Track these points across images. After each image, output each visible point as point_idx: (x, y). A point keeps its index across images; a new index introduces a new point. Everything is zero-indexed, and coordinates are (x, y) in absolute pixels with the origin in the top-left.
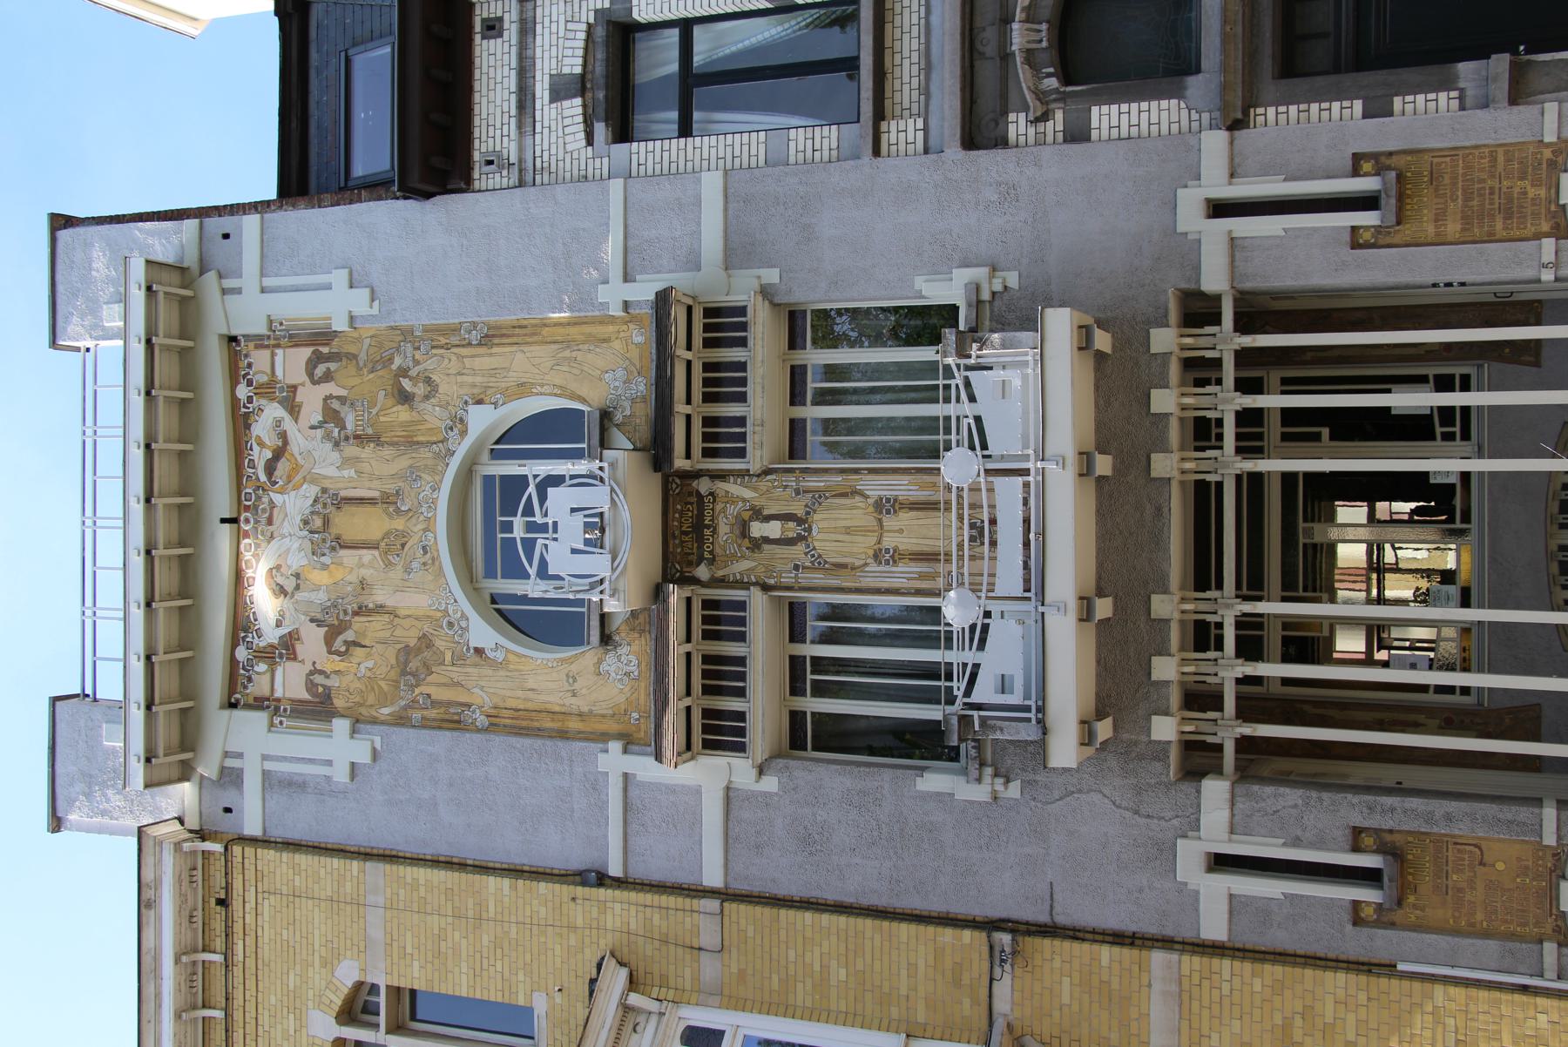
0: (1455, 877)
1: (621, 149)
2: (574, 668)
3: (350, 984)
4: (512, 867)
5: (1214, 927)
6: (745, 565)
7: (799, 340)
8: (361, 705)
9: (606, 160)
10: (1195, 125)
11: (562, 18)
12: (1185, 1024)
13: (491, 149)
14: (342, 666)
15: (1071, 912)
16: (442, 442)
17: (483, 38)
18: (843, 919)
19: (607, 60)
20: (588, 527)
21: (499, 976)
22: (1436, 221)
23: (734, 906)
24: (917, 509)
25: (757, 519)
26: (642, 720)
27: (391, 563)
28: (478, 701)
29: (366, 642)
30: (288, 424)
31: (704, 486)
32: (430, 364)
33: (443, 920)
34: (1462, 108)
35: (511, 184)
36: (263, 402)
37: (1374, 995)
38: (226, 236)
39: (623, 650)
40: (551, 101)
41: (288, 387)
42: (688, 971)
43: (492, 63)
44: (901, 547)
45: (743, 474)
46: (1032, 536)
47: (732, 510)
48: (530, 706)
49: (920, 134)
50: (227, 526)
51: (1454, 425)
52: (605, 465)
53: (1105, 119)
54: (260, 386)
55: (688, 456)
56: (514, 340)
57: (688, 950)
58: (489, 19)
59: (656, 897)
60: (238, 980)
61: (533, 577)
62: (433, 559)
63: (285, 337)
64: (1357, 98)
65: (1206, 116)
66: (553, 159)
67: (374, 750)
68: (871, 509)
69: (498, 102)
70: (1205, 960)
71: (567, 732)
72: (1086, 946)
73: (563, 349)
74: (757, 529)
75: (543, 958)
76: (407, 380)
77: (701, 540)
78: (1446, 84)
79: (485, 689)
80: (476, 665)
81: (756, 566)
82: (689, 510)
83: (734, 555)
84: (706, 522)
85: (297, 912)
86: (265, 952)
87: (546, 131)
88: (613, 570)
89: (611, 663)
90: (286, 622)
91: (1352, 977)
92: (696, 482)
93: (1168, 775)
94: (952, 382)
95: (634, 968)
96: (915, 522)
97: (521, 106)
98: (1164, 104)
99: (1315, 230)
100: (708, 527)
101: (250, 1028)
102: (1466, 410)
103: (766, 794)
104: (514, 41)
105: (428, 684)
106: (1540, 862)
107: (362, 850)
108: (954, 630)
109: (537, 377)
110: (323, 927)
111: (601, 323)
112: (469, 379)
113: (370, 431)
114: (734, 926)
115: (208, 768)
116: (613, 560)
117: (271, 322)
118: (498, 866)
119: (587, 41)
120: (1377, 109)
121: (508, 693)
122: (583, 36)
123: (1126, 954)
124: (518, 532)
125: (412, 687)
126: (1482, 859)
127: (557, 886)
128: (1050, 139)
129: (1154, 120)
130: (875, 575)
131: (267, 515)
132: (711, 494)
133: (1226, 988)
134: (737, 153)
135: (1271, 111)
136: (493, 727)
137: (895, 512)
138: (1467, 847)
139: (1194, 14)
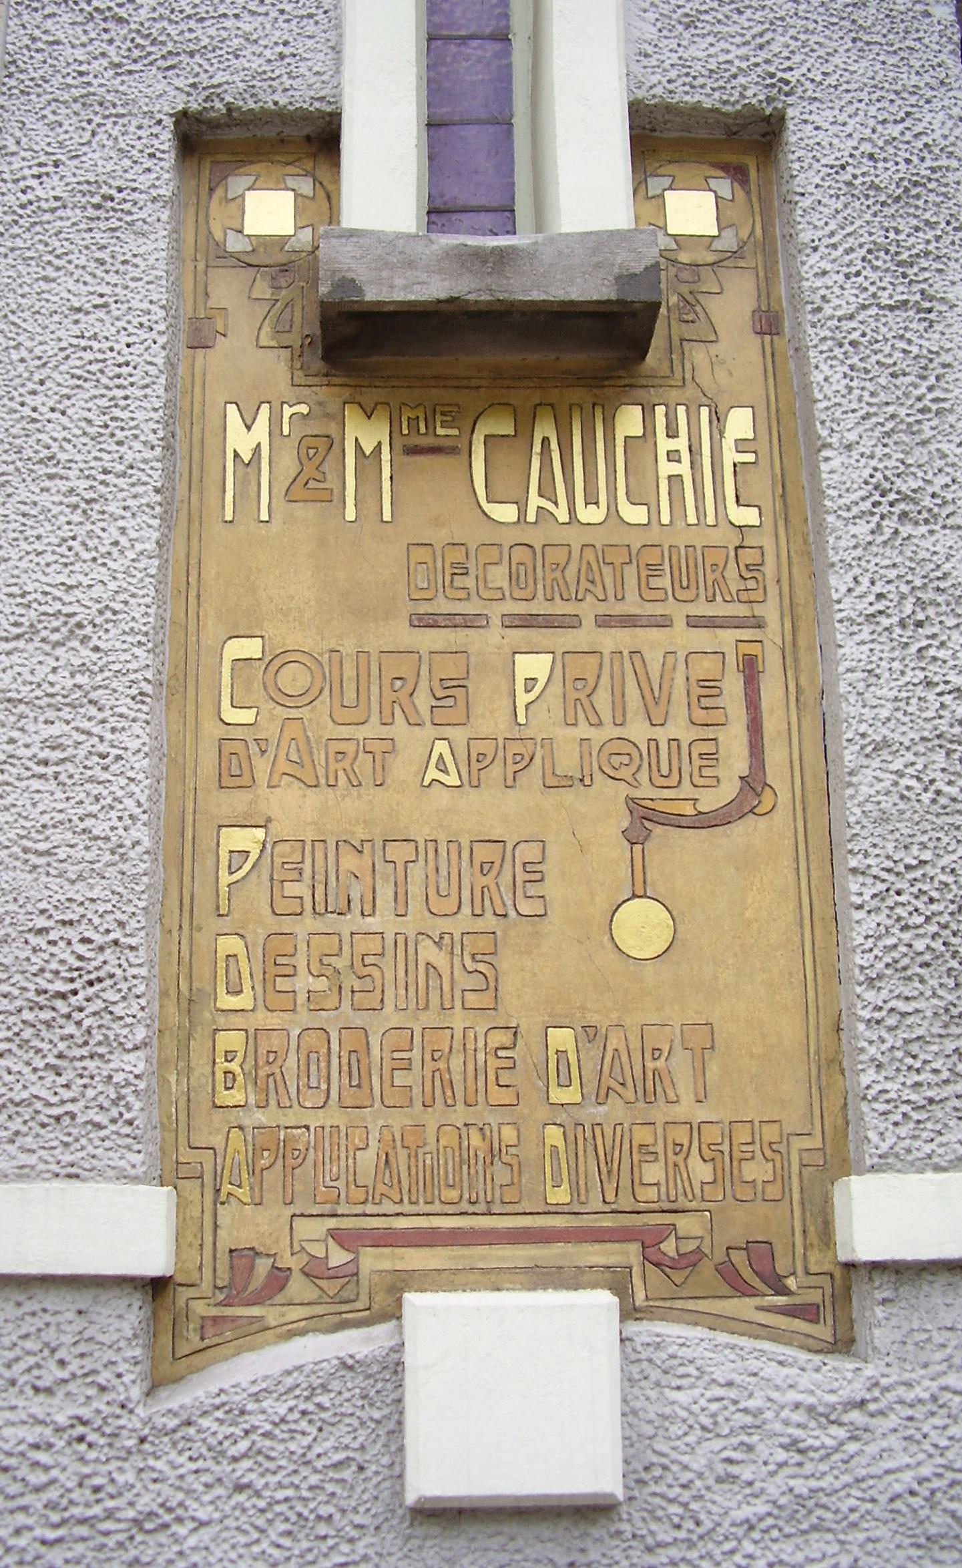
106: (701, 1171)
126: (677, 822)
138: (734, 740)
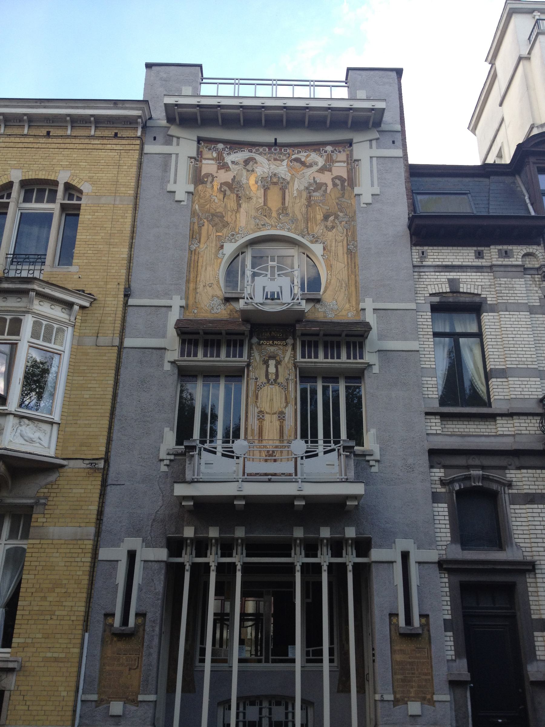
0: (124, 658)
1: (428, 307)
2: (215, 286)
3: (81, 188)
4: (132, 259)
5: (104, 554)
7: (349, 381)
9: (423, 302)
10: (440, 548)
11: (483, 284)
12: (63, 542)
13: (429, 254)
15: (112, 493)
17: (475, 250)
18: (111, 397)
19: (465, 303)
20: (273, 294)
21: (85, 252)
22: (401, 650)
23: (116, 351)
24: (280, 429)
25: (276, 363)
28: (201, 246)
29: (225, 200)
30: (315, 168)
31: (290, 341)
32: (340, 228)
33: (109, 229)
34: (448, 661)
35: (415, 263)
36: (325, 157)
37: (75, 623)
38: (393, 142)
39: (222, 307)
40: (448, 279)
42: (88, 331)
43: (464, 254)
44: (265, 422)
45: (295, 356)
46: (270, 477)
47: (280, 352)
48: (200, 268)
49: (434, 432)
50: (274, 141)
51: (313, 656)
52: (300, 301)
53: (442, 509)
54: (331, 156)
55: (303, 335)
57: (97, 331)
58: (483, 253)
59: (120, 319)
60: (83, 141)
61: (253, 270)
62: (260, 229)
64: (452, 616)
65: (444, 552)
66: (424, 280)
67: (181, 201)
68: (280, 410)
69: (448, 257)
70: (90, 551)
72: (97, 499)
74: (272, 363)
75: (93, 270)
77: (268, 339)
78: (458, 655)
80: (216, 245)
85: (112, 167)
86: (95, 153)
87: (436, 277)
88: (256, 304)
89: (217, 301)
90: (234, 166)
91: (83, 614)
93: (169, 534)
94: (332, 444)
95: (89, 309)
96: (275, 428)
97: (446, 266)
98: (449, 535)
99: (397, 598)
100: (273, 343)
101: (63, 146)
102: (321, 661)
103: (162, 366)
104: (474, 264)
105: (208, 225)
107: (138, 195)
108: (230, 445)
110: (106, 178)
111: (357, 300)
112: (333, 245)
113: (312, 202)
114: (107, 351)
115: (174, 131)
116: (261, 304)
117: (358, 160)
118: (132, 253)
119: (473, 294)
120: (448, 625)
121: (205, 259)
122: (476, 292)
123: (93, 517)
124: (271, 263)
125: (207, 218)
127: (124, 277)
128: (433, 486)
129: (442, 530)
130: (253, 411)
132: (287, 344)
133: (78, 559)
134: (427, 356)
135: (446, 580)
136: (191, 252)
137: (279, 420)
138: (137, 663)
139: (486, 548)
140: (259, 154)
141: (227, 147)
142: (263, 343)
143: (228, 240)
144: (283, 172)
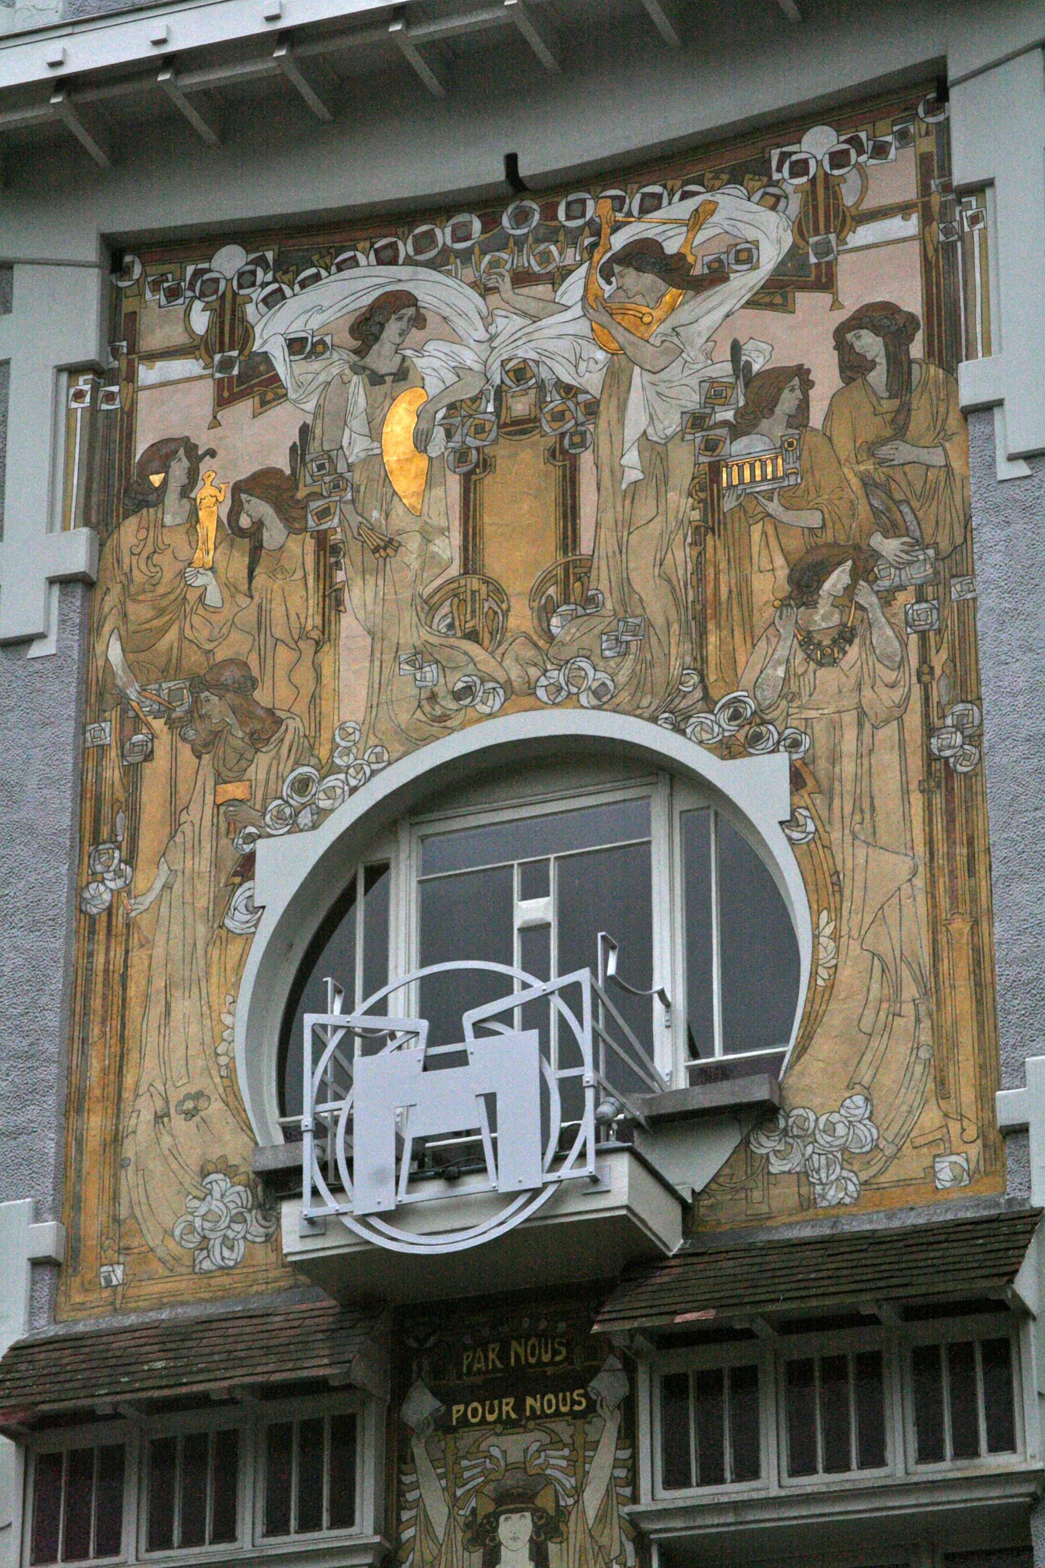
6: (438, 1511)
8: (125, 589)
14: (208, 525)
16: (706, 697)
25: (537, 1529)
26: (106, 1294)
27: (433, 609)
28: (141, 884)
29: (260, 579)
32: (884, 636)
41: (829, 264)
48: (135, 1010)
56: (941, 848)
62: (443, 718)
63: (947, 232)
67: (25, 641)
71: (79, 1111)
73: (919, 980)
76: (846, 580)
79: (166, 895)
80: (217, 863)
81: (434, 1539)
82: (555, 1353)
83: (458, 1480)
84: (529, 1401)
92: (620, 1366)
100: (519, 1408)
109: (856, 919)
112: (849, 744)
113: (728, 504)
117: (980, 188)
121: (159, 952)
125: (165, 711)
131: (536, 268)
132: (591, 1407)
140: (432, 265)
141: (261, 261)
142: (464, 1422)
143: (279, 817)
144: (563, 346)
